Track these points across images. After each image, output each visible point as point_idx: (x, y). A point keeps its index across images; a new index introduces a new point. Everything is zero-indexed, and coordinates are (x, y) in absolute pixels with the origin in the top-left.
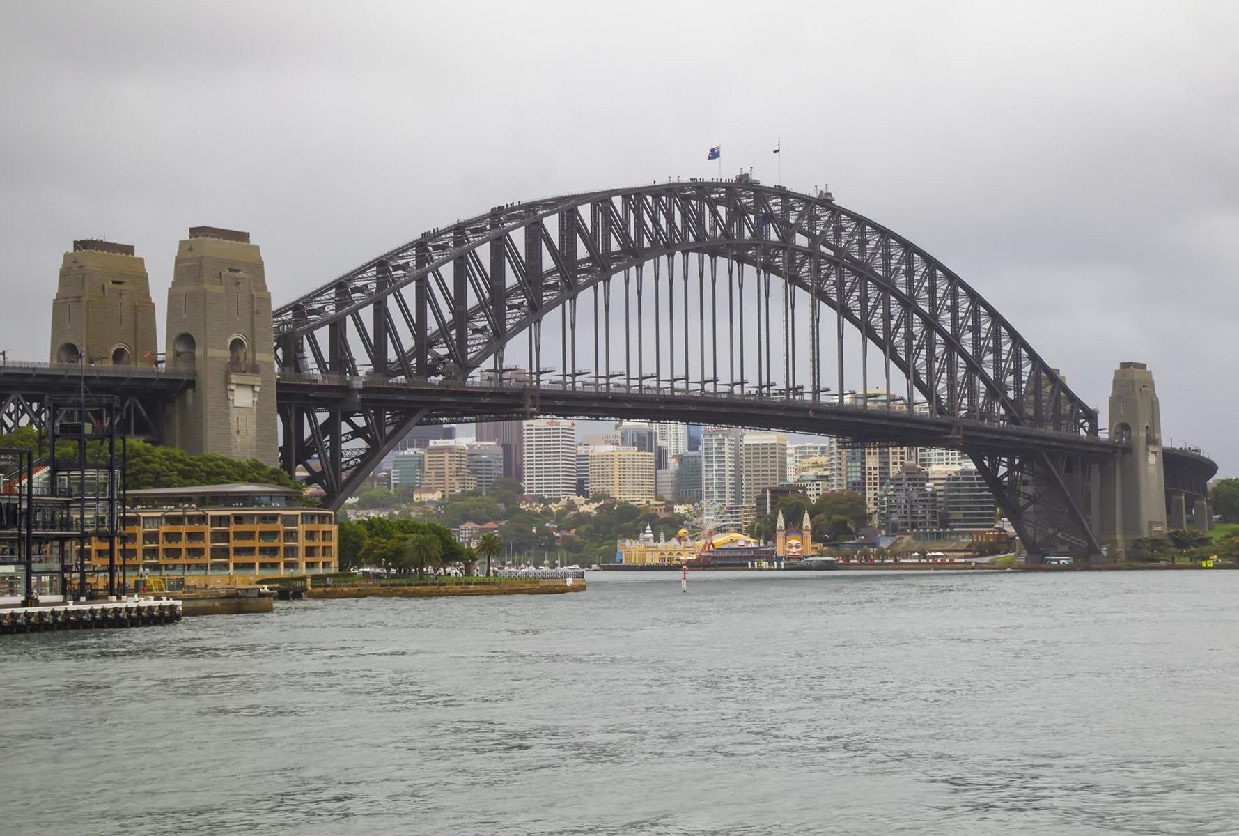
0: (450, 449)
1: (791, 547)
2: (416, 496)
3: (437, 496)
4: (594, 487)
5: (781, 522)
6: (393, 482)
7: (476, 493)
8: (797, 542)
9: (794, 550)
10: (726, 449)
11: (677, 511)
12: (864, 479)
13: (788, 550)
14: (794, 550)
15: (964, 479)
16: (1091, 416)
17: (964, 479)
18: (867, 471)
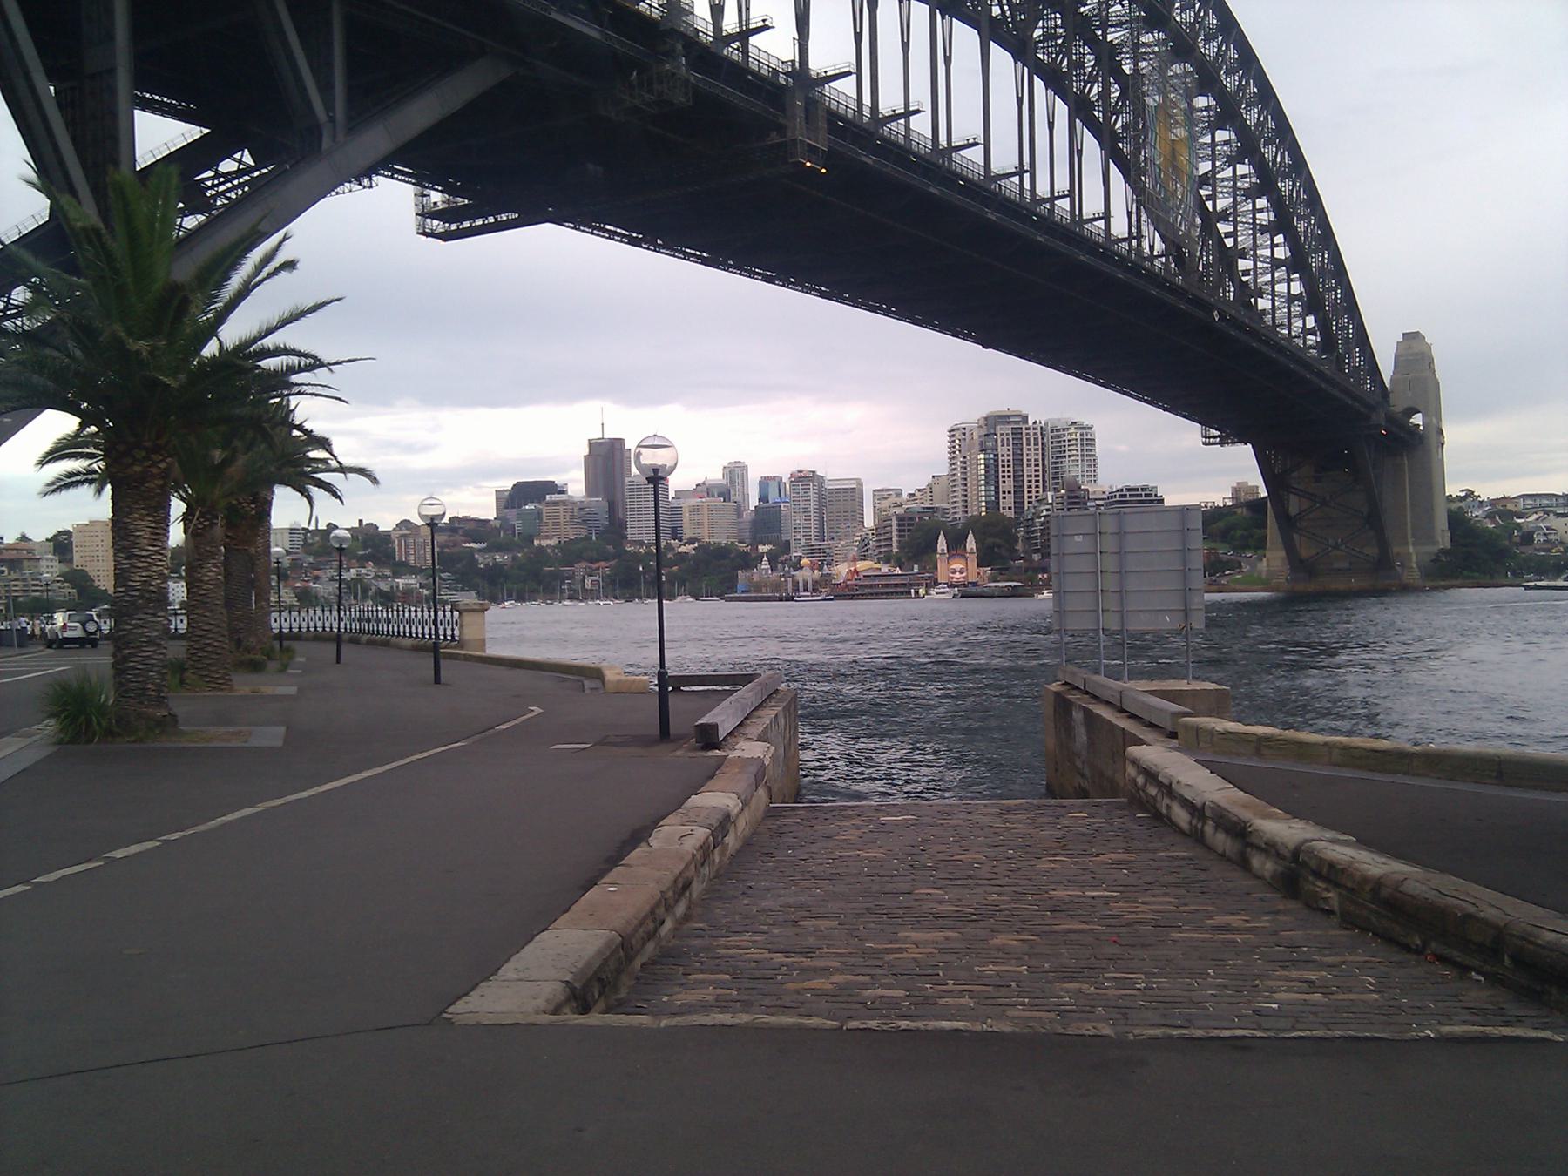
0: (564, 502)
1: (954, 572)
2: (536, 543)
3: (553, 542)
4: (688, 533)
5: (942, 544)
6: (516, 532)
7: (588, 538)
8: (961, 566)
9: (958, 575)
10: (811, 493)
11: (761, 551)
12: (999, 503)
13: (951, 575)
14: (958, 575)
18: (1001, 495)
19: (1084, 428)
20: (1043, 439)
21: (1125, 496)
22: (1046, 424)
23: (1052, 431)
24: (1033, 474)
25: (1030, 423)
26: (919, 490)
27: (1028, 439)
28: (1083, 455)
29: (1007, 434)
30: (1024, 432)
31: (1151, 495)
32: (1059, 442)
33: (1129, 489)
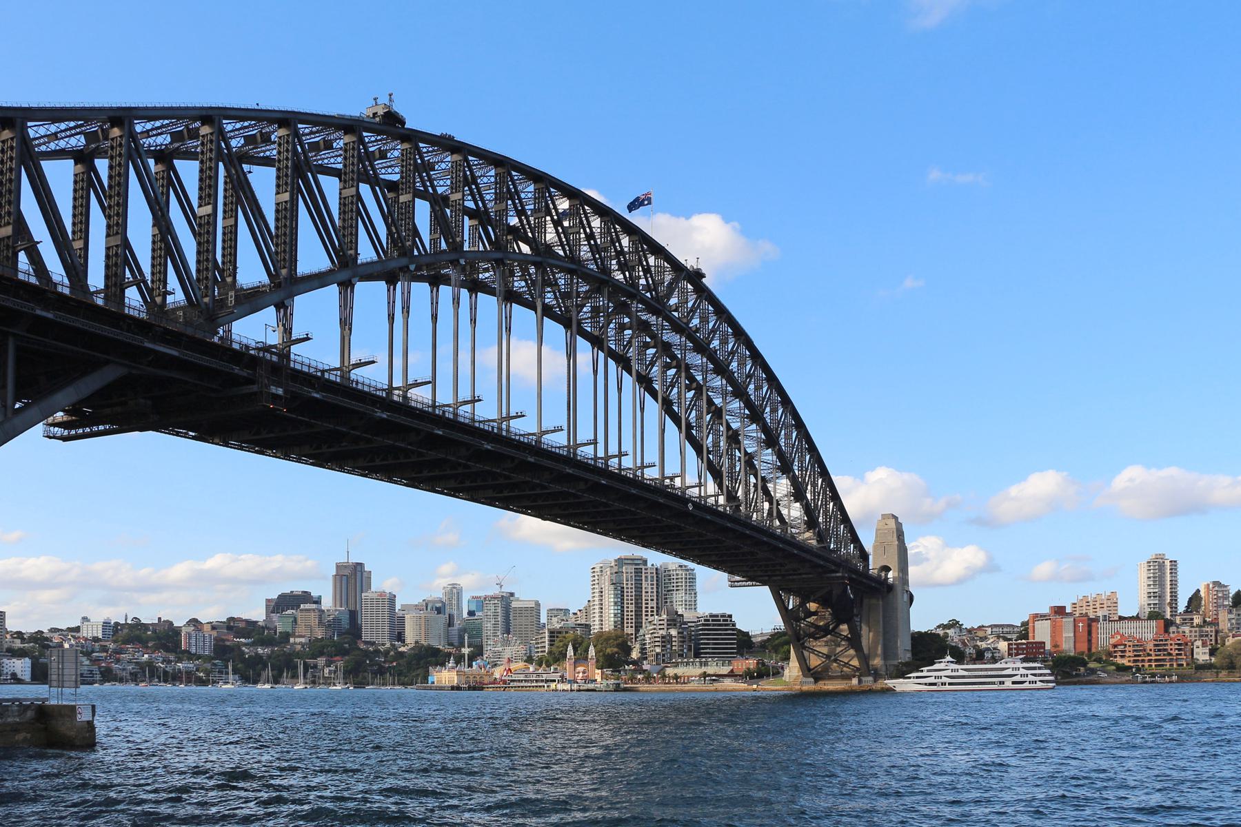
2: (292, 640)
5: (570, 652)
15: (713, 620)
16: (864, 556)
17: (713, 620)
19: (688, 570)
20: (657, 577)
21: (708, 621)
22: (661, 566)
23: (665, 572)
24: (649, 602)
25: (649, 565)
26: (580, 611)
27: (646, 577)
28: (686, 590)
29: (631, 573)
30: (643, 571)
31: (727, 621)
32: (670, 580)
33: (711, 616)
